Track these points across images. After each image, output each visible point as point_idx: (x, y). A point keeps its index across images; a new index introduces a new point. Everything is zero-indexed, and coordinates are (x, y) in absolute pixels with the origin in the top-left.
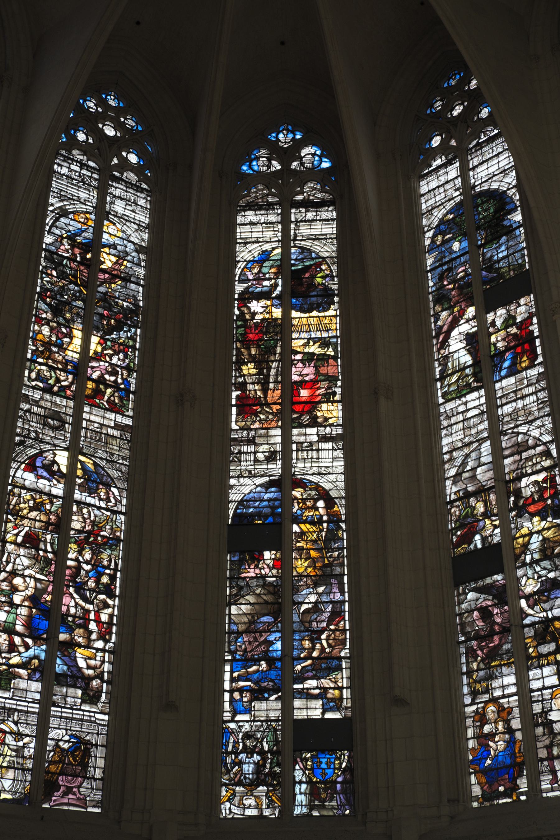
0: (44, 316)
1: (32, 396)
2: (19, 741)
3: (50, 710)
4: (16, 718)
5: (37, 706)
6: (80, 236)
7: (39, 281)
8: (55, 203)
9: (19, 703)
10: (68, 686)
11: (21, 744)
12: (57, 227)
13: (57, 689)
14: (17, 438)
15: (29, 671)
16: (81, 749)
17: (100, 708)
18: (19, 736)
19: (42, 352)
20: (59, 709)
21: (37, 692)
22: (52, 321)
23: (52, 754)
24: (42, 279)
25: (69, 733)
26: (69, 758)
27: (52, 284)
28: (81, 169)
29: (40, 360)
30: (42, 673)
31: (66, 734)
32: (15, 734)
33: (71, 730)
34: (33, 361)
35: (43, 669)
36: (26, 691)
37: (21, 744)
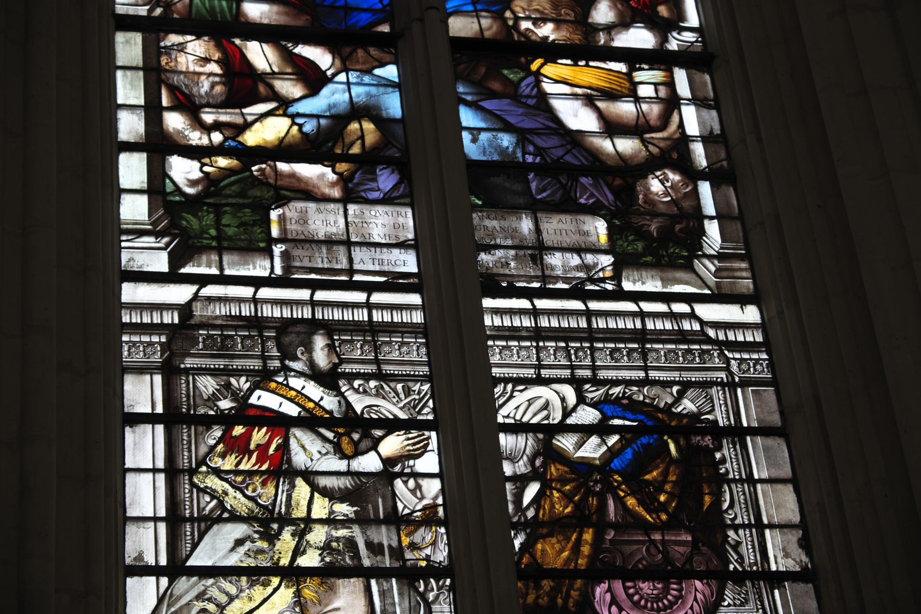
2: (358, 453)
3: (481, 311)
4: (322, 358)
5: (415, 299)
9: (320, 295)
10: (536, 208)
11: (369, 463)
13: (488, 224)
15: (342, 167)
16: (668, 459)
17: (712, 280)
18: (353, 431)
20: (524, 304)
21: (402, 245)
23: (532, 490)
25: (594, 393)
26: (620, 502)
30: (402, 167)
31: (581, 399)
32: (330, 422)
33: (596, 382)
35: (406, 151)
36: (348, 244)
37: (369, 463)
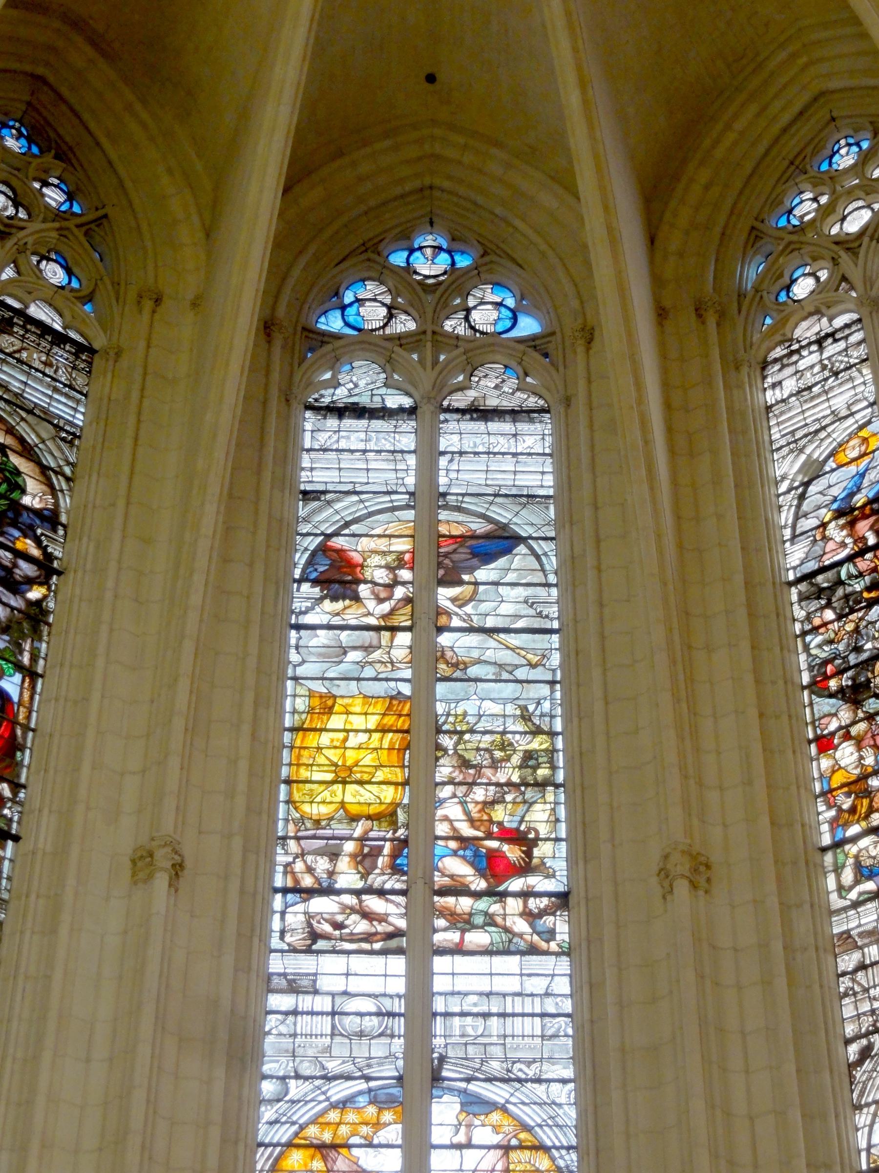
0: (833, 725)
1: (860, 926)
6: (859, 489)
7: (803, 657)
8: (787, 467)
12: (805, 515)
14: (853, 1050)
19: (853, 810)
22: (854, 723)
24: (807, 648)
27: (831, 642)
28: (821, 349)
29: (854, 830)
34: (838, 845)
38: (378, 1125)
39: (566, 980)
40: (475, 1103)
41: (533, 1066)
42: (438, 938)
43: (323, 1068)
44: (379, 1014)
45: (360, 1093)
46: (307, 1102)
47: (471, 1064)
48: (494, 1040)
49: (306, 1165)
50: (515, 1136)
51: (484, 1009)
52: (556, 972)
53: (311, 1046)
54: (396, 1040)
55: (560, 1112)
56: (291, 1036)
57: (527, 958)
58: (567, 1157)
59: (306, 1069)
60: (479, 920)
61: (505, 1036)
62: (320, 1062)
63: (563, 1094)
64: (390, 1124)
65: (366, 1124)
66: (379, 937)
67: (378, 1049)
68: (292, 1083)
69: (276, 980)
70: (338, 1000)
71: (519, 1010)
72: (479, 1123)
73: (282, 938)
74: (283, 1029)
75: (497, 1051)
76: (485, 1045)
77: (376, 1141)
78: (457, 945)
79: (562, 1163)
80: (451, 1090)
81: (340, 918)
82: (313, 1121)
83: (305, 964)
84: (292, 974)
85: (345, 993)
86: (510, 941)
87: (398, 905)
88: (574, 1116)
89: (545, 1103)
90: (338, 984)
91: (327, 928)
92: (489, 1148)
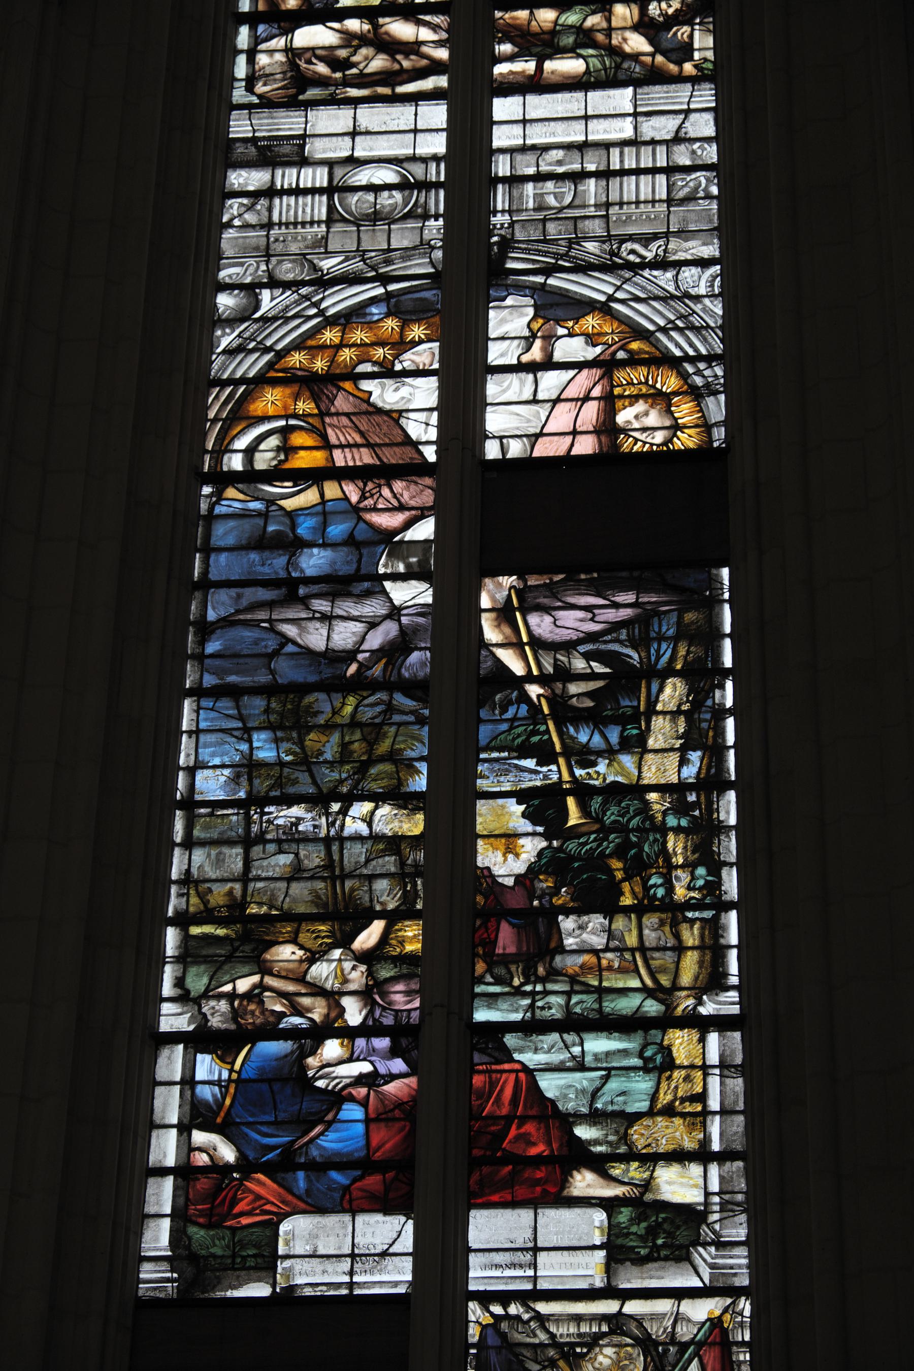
38: (402, 345)
39: (709, 117)
40: (558, 305)
41: (654, 246)
42: (500, 69)
43: (315, 268)
44: (403, 186)
45: (373, 301)
46: (288, 320)
47: (553, 248)
48: (591, 211)
49: (285, 407)
50: (622, 348)
51: (577, 167)
52: (692, 106)
53: (295, 239)
54: (432, 222)
55: (698, 308)
56: (263, 224)
57: (646, 89)
58: (706, 373)
59: (287, 271)
60: (569, 40)
61: (608, 205)
62: (310, 262)
63: (699, 281)
64: (421, 342)
65: (382, 344)
66: (405, 76)
67: (402, 237)
68: (266, 294)
69: (240, 149)
70: (339, 172)
71: (630, 164)
72: (565, 332)
73: (250, 88)
74: (250, 218)
75: (596, 227)
76: (575, 219)
77: (398, 367)
78: (531, 77)
79: (699, 381)
80: (520, 289)
81: (343, 53)
82: (298, 345)
83: (289, 123)
84: (264, 138)
85: (352, 161)
86: (618, 67)
87: (434, 28)
88: (720, 312)
89: (673, 297)
90: (341, 149)
91: (322, 69)
92: (579, 366)
